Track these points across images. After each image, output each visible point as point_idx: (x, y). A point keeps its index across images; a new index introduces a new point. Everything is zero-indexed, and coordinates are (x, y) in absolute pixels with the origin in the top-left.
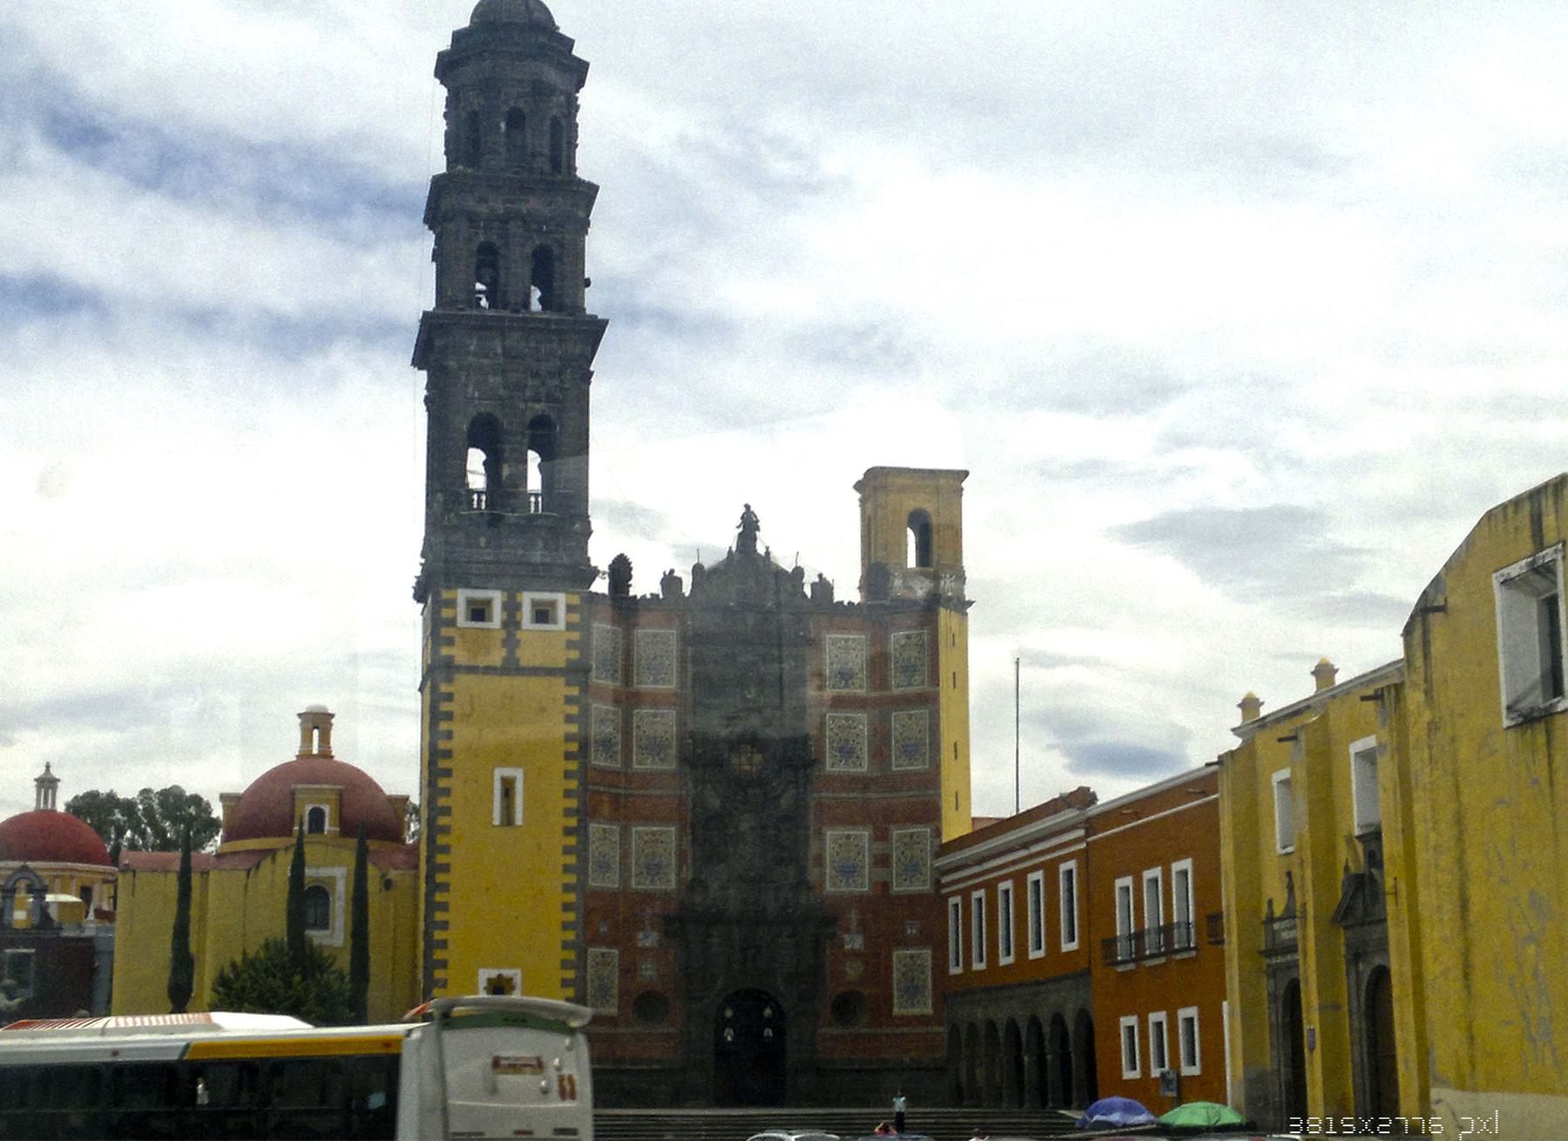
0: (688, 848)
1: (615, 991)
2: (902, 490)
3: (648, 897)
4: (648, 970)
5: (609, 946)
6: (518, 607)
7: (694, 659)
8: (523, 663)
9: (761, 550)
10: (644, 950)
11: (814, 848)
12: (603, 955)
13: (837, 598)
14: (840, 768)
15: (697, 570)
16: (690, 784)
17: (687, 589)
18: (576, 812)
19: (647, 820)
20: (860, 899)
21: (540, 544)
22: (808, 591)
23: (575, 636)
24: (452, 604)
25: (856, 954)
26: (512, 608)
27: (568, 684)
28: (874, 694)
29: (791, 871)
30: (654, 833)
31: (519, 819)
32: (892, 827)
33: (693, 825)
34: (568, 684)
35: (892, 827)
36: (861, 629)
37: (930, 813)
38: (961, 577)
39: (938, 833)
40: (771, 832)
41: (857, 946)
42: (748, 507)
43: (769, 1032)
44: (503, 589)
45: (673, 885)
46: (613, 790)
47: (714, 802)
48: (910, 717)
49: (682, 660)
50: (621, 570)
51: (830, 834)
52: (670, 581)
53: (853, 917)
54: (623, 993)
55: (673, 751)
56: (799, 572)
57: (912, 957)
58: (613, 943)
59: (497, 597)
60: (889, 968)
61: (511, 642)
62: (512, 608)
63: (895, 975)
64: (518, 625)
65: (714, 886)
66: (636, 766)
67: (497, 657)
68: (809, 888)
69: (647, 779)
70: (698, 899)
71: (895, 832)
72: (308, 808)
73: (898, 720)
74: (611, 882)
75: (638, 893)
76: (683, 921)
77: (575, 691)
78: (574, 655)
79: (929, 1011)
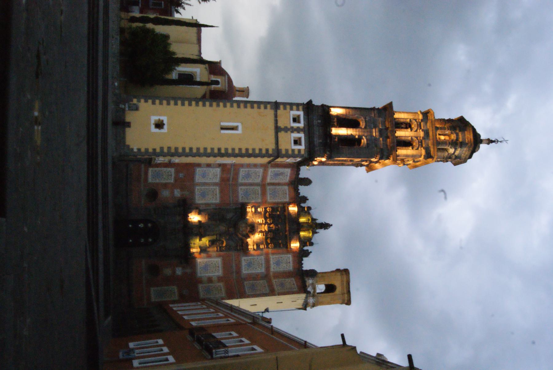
2: (342, 281)
3: (193, 192)
4: (165, 193)
5: (175, 177)
6: (299, 132)
8: (279, 134)
9: (317, 231)
13: (304, 259)
14: (244, 263)
15: (309, 208)
17: (303, 205)
19: (221, 191)
20: (194, 273)
21: (321, 141)
22: (305, 248)
23: (290, 152)
24: (298, 110)
25: (174, 272)
26: (298, 130)
27: (273, 149)
28: (271, 274)
30: (216, 195)
31: (223, 132)
34: (273, 149)
36: (294, 268)
37: (231, 296)
38: (314, 306)
42: (332, 225)
44: (304, 127)
46: (231, 179)
49: (278, 203)
50: (307, 182)
51: (219, 260)
52: (305, 199)
53: (188, 271)
56: (312, 244)
58: (176, 180)
59: (301, 125)
61: (286, 129)
62: (298, 130)
63: (166, 288)
64: (292, 132)
66: (240, 187)
67: (280, 124)
69: (235, 192)
71: (221, 284)
72: (219, 80)
74: (198, 178)
77: (270, 152)
78: (284, 152)
79: (153, 300)
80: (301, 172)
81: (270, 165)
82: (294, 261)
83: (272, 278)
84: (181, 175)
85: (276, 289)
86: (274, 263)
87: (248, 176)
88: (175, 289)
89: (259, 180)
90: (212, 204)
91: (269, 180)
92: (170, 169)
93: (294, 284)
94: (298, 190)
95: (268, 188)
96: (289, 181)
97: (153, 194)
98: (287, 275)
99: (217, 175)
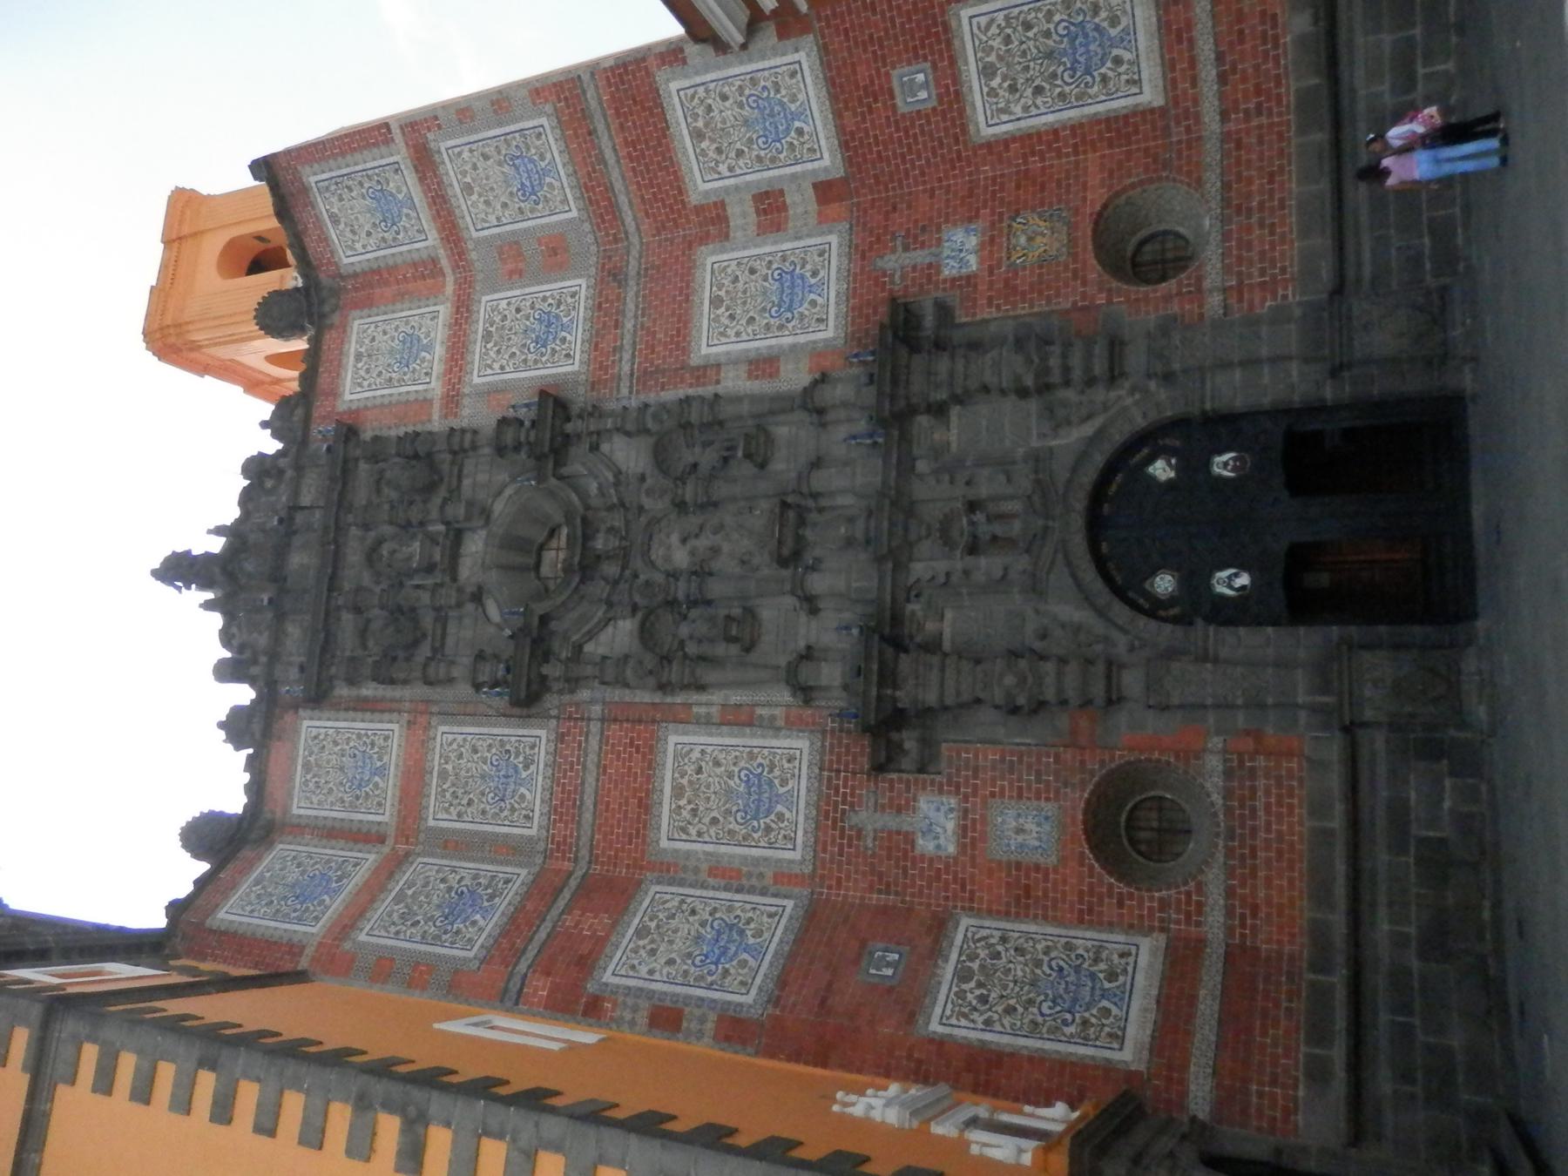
0: (710, 702)
1: (1085, 938)
3: (830, 817)
5: (936, 953)
7: (351, 682)
9: (216, 545)
10: (971, 832)
11: (734, 382)
12: (963, 975)
14: (577, 337)
15: (227, 672)
16: (584, 694)
17: (244, 694)
18: (363, 1104)
19: (646, 804)
25: (989, 243)
28: (450, 288)
29: (782, 432)
30: (678, 792)
32: (694, 199)
33: (663, 687)
35: (694, 199)
36: (344, 328)
39: (670, 54)
40: (689, 492)
41: (973, 241)
42: (156, 574)
43: (1223, 464)
45: (801, 745)
46: (567, 894)
47: (621, 635)
48: (468, 189)
51: (707, 345)
52: (238, 727)
53: (895, 262)
54: (1087, 916)
55: (511, 732)
57: (987, 72)
58: (940, 927)
60: (1029, 141)
65: (809, 631)
68: (823, 379)
69: (563, 805)
70: (831, 674)
71: (701, 185)
73: (484, 221)
74: (773, 923)
75: (818, 846)
76: (888, 731)
80: (184, 889)
81: (304, 964)
82: (337, 374)
83: (445, 263)
84: (885, 964)
85: (411, 178)
86: (428, 348)
87: (460, 904)
88: (987, 124)
89: (424, 867)
90: (706, 722)
91: (371, 859)
92: (967, 1032)
93: (335, 220)
94: (248, 788)
95: (386, 817)
96: (271, 845)
97: (1130, 831)
98: (374, 286)
99: (641, 932)
